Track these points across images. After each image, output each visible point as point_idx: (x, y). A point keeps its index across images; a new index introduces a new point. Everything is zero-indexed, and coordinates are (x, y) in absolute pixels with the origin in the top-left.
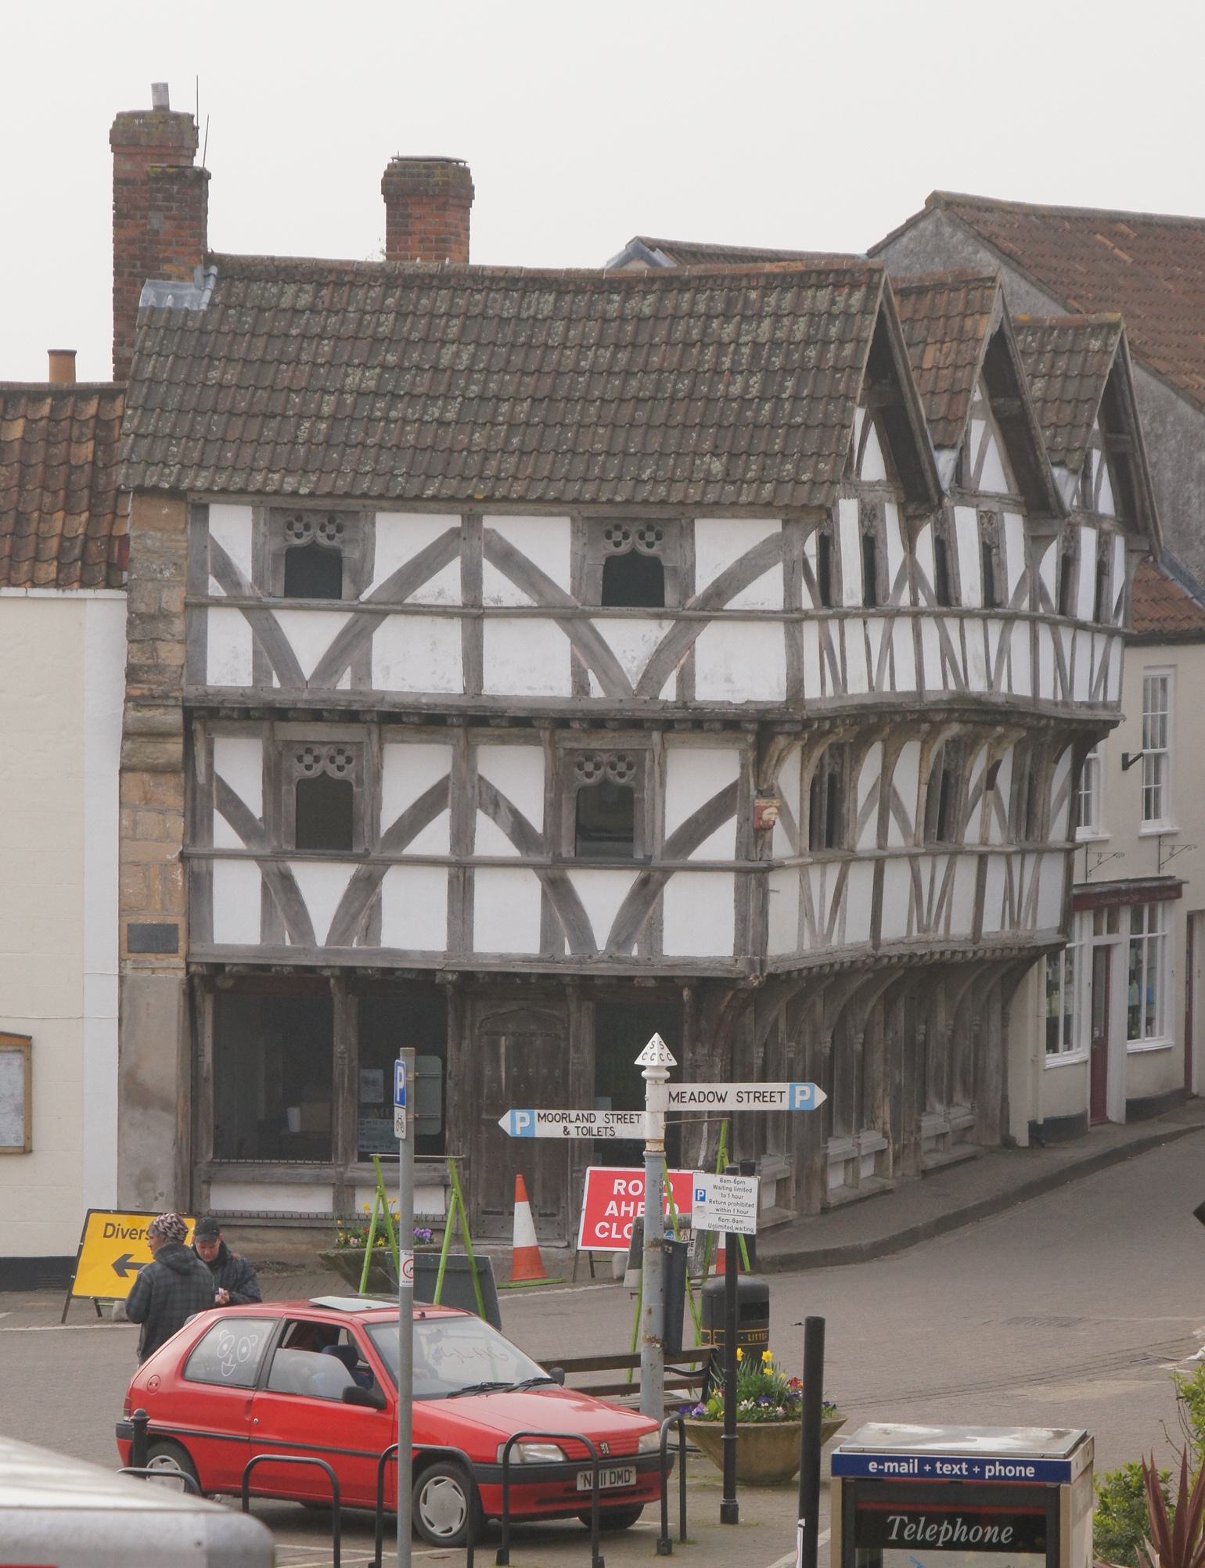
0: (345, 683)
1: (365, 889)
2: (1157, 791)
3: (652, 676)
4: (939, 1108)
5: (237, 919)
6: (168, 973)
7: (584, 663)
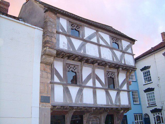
0: (82, 51)
1: (80, 91)
5: (59, 96)
6: (48, 107)
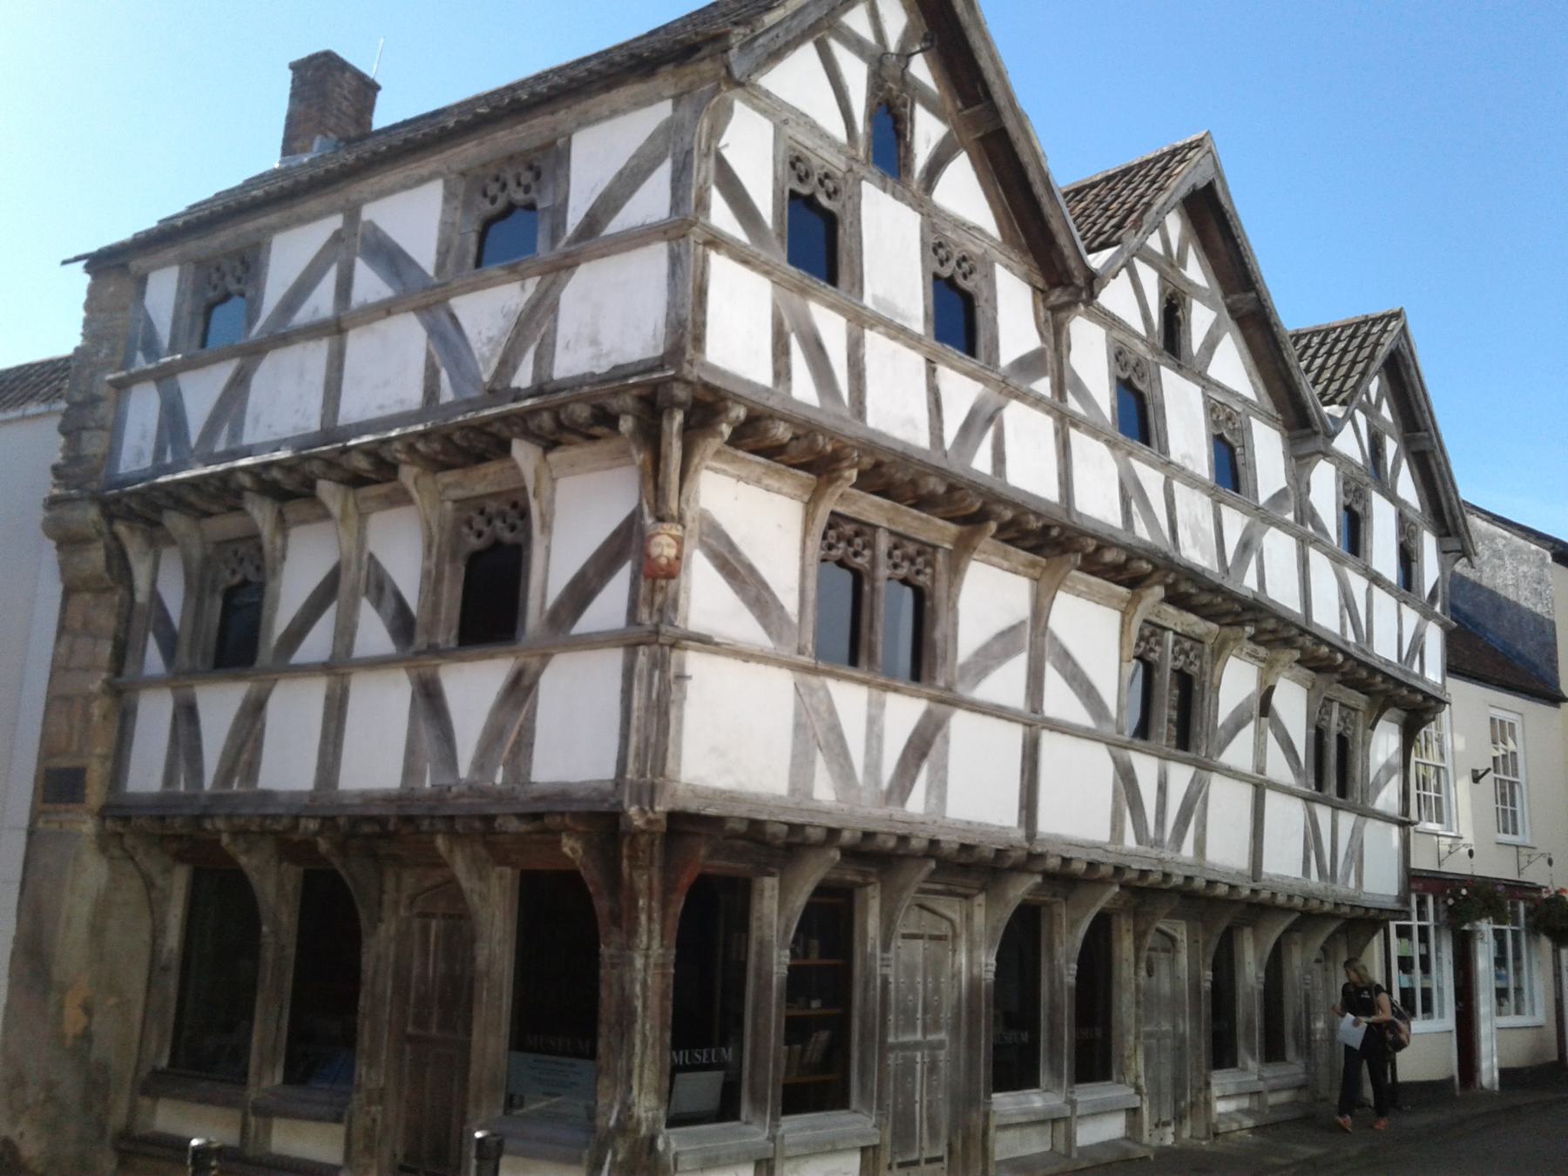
2: (1514, 813)
3: (508, 363)
4: (1253, 1065)
7: (438, 360)
